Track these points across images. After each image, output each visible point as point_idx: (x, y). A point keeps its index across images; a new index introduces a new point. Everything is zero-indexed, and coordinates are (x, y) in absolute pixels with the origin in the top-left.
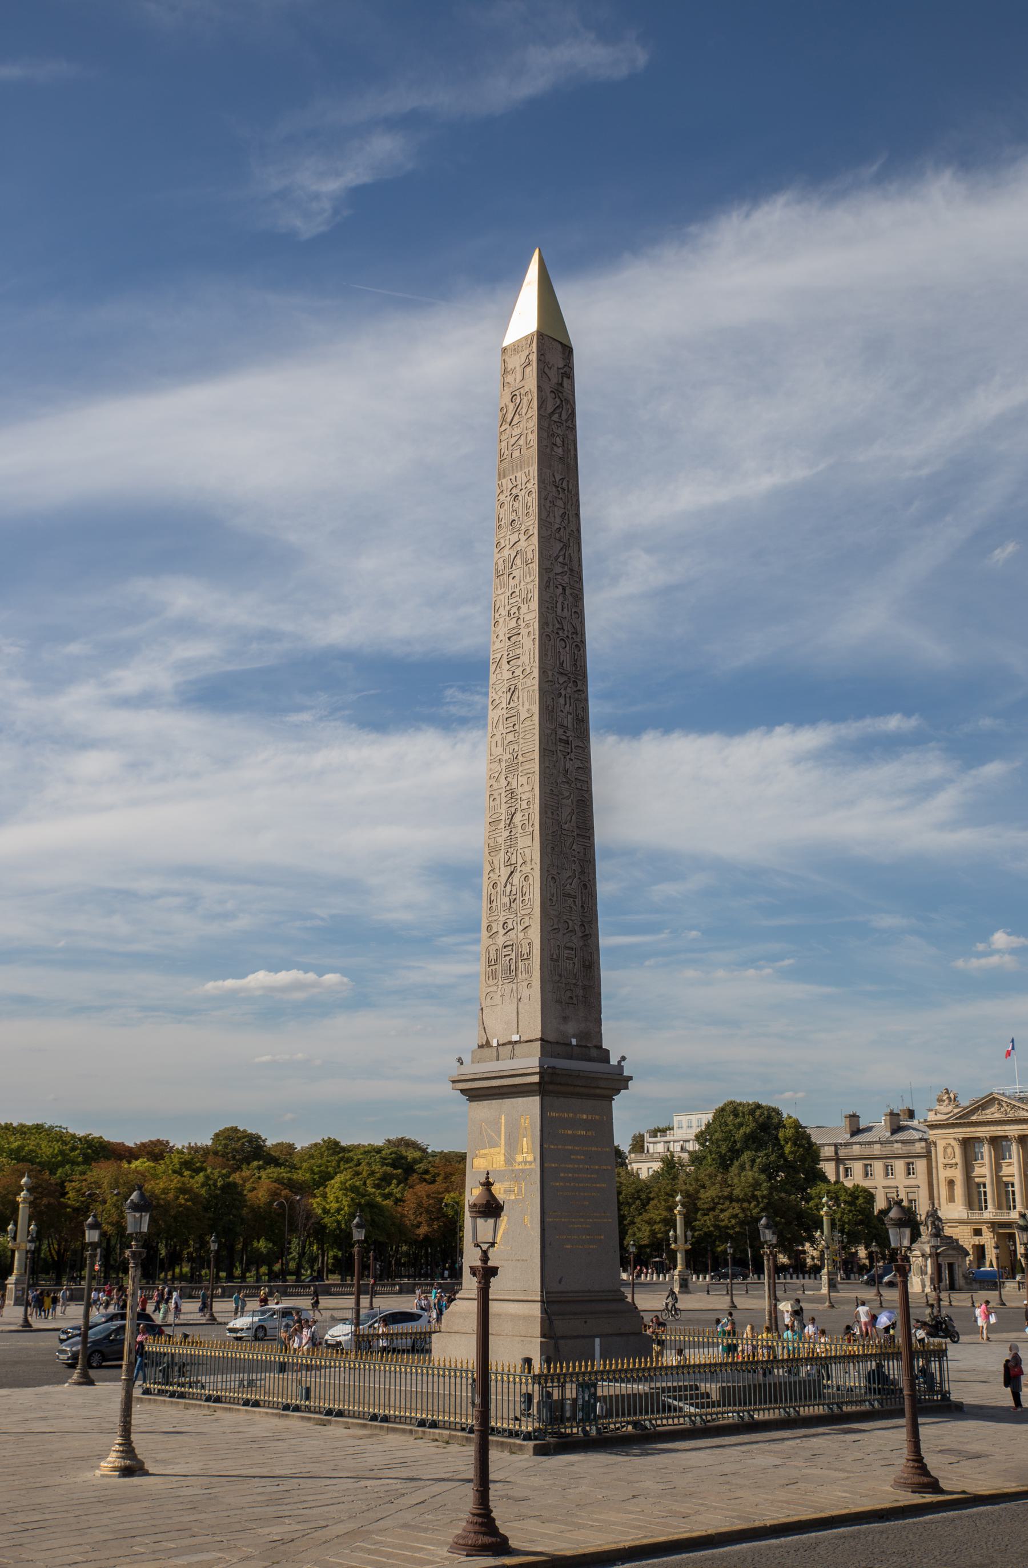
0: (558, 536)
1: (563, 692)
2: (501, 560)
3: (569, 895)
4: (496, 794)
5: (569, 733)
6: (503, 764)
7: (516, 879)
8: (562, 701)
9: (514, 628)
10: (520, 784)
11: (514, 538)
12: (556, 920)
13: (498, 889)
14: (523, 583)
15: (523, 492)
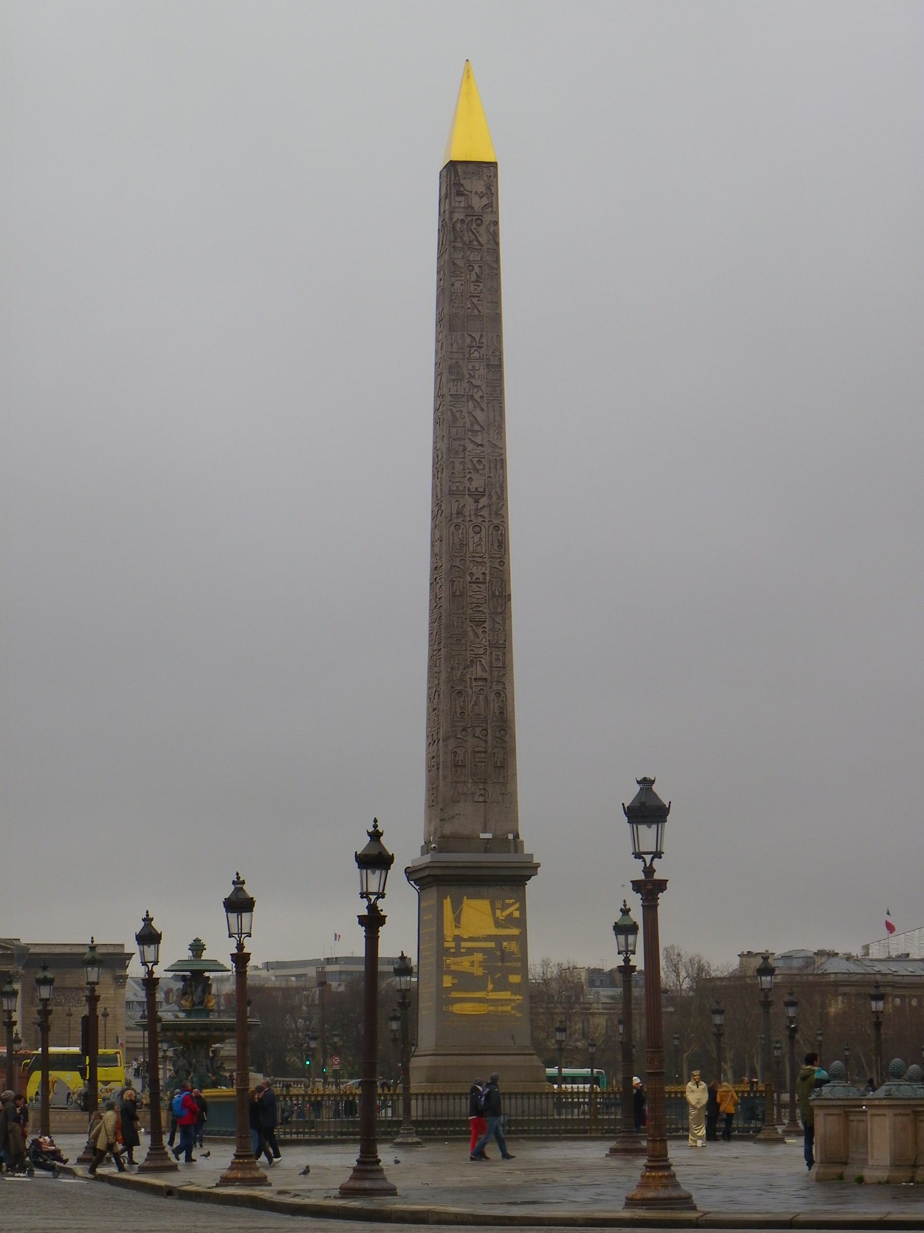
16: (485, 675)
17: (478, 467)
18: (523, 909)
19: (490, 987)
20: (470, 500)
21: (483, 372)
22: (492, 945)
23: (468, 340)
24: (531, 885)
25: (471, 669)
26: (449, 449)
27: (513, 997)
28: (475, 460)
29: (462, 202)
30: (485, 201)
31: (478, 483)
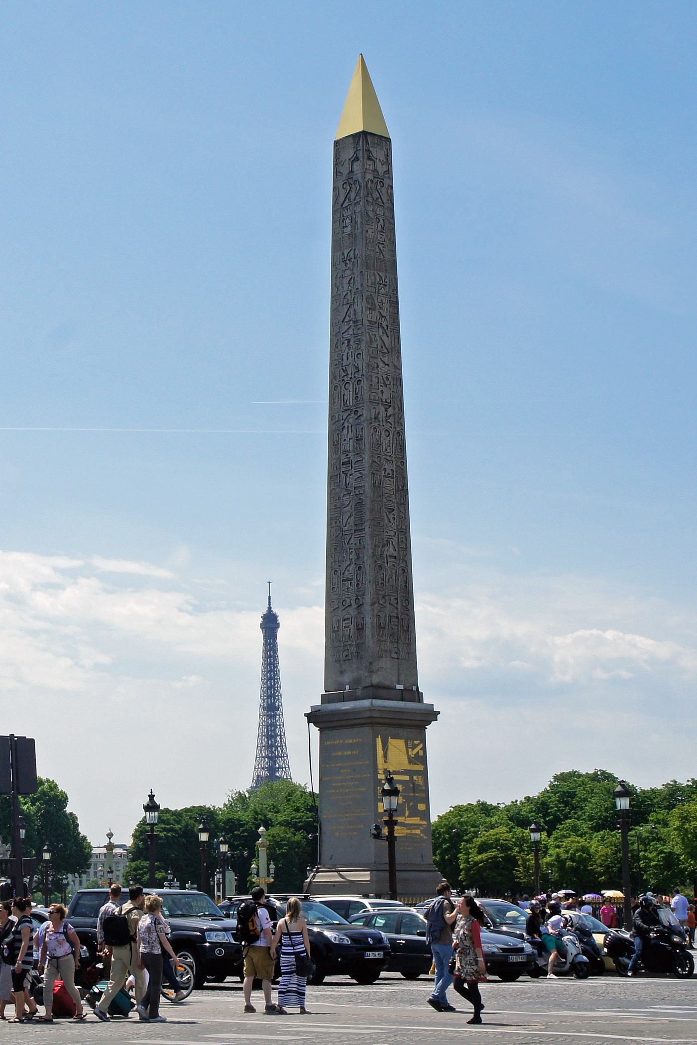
0: (345, 301)
1: (346, 424)
3: (348, 580)
5: (350, 455)
8: (345, 431)
12: (336, 602)
16: (395, 554)
17: (388, 383)
18: (424, 749)
19: (407, 814)
20: (382, 409)
21: (386, 305)
22: (407, 778)
23: (378, 277)
24: (431, 730)
25: (387, 548)
26: (368, 365)
27: (421, 822)
28: (385, 376)
29: (369, 165)
30: (385, 168)
31: (386, 396)
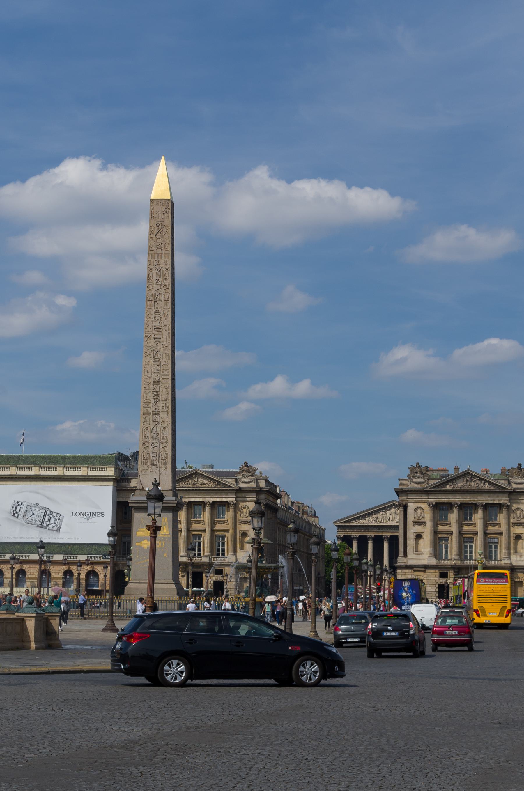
2: (150, 294)
4: (147, 392)
6: (152, 381)
7: (159, 427)
9: (158, 325)
10: (161, 390)
11: (158, 287)
13: (149, 430)
14: (162, 308)
15: (163, 269)
